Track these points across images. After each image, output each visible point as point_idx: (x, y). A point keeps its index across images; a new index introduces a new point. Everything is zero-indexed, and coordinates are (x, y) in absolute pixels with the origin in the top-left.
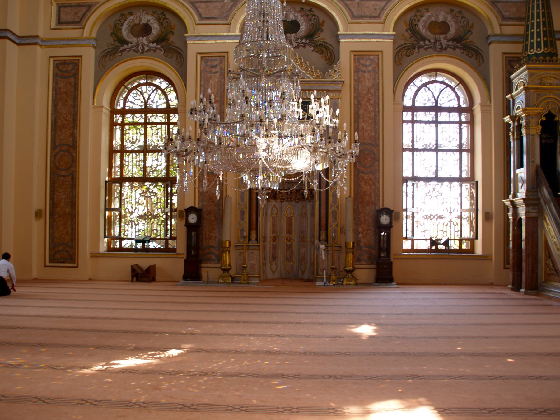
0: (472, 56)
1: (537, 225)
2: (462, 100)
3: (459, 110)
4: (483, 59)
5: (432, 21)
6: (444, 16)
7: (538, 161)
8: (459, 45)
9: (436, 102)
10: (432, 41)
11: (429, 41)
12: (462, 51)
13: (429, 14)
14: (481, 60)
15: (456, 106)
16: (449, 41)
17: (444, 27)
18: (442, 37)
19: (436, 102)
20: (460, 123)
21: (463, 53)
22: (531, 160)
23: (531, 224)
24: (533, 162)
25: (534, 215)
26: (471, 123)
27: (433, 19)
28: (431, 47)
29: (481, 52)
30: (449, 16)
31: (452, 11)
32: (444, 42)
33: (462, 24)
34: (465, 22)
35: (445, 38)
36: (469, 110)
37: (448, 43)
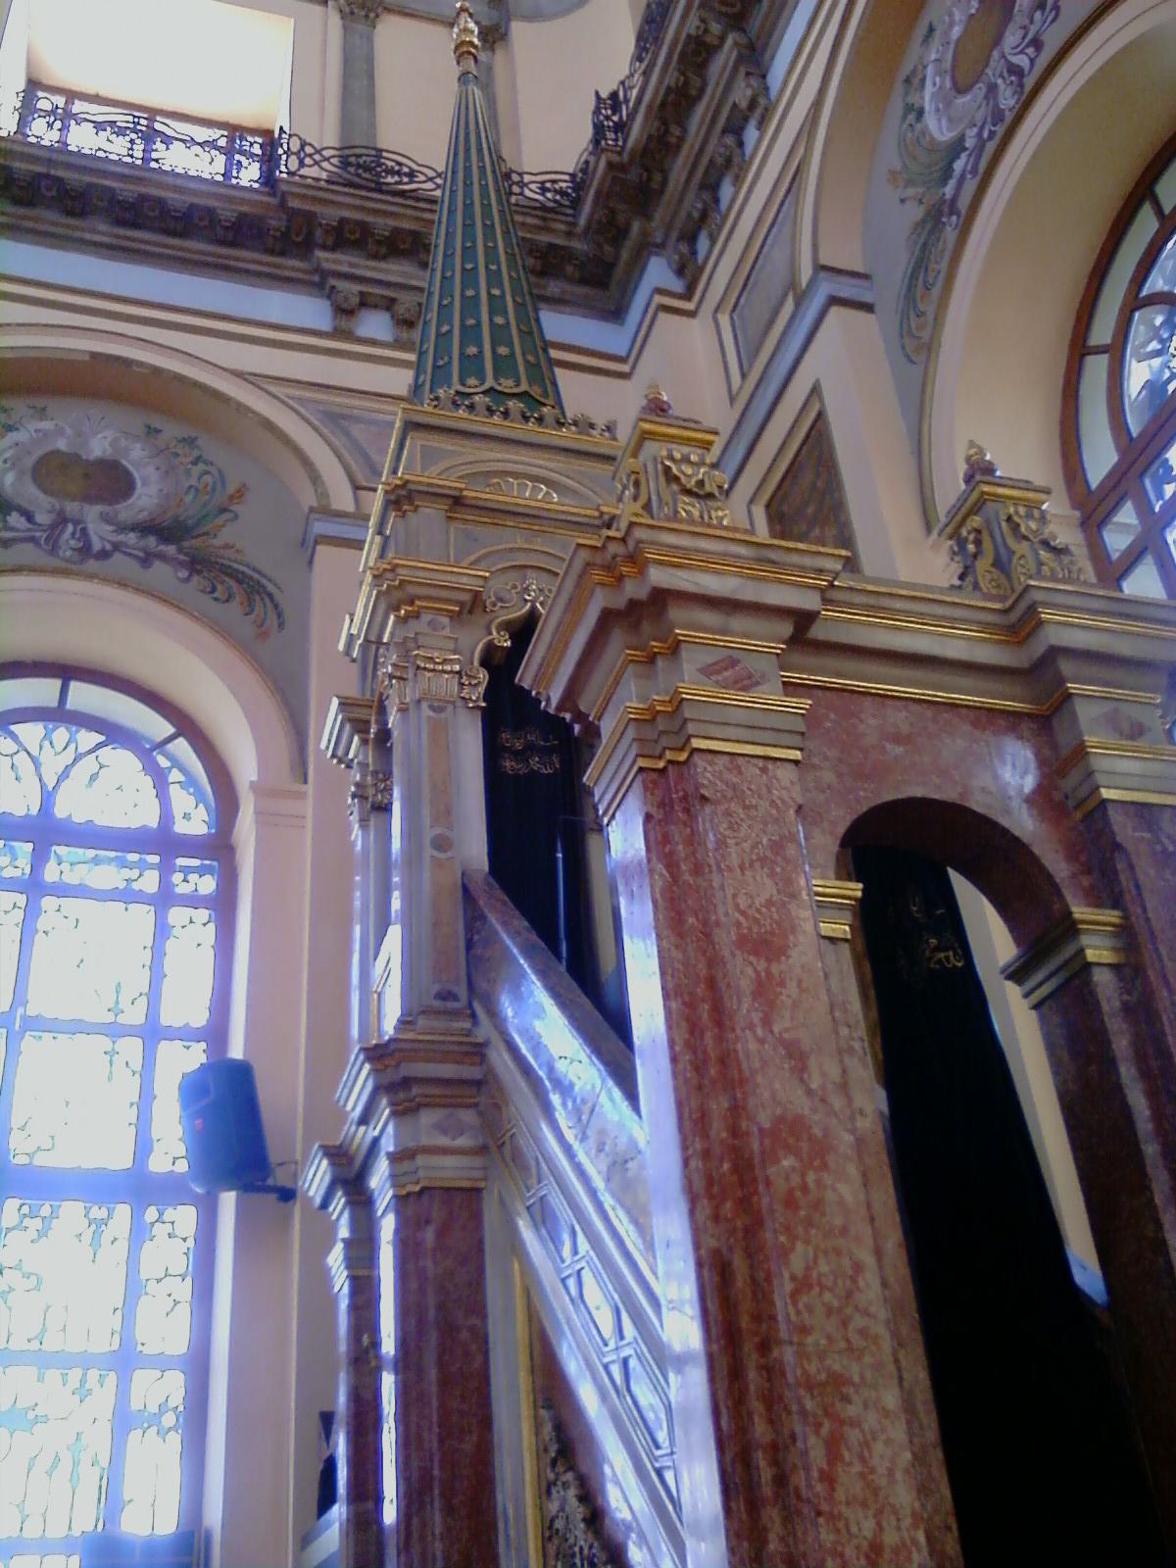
0: (227, 601)
1: (479, 1247)
2: (181, 800)
3: (163, 843)
4: (279, 615)
5: (56, 453)
6: (114, 443)
7: (474, 846)
8: (171, 550)
9: (48, 798)
10: (43, 518)
11: (29, 517)
12: (183, 574)
13: (47, 425)
14: (272, 617)
15: (153, 822)
16: (122, 528)
17: (110, 481)
18: (92, 513)
19: (48, 798)
20: (164, 899)
21: (187, 580)
22: (428, 835)
23: (429, 1235)
24: (441, 844)
25: (451, 1170)
26: (223, 906)
27: (62, 445)
28: (33, 540)
29: (270, 587)
30: (139, 445)
31: (152, 432)
32: (100, 533)
33: (193, 482)
34: (207, 478)
35: (105, 519)
36: (218, 849)
37: (121, 538)
